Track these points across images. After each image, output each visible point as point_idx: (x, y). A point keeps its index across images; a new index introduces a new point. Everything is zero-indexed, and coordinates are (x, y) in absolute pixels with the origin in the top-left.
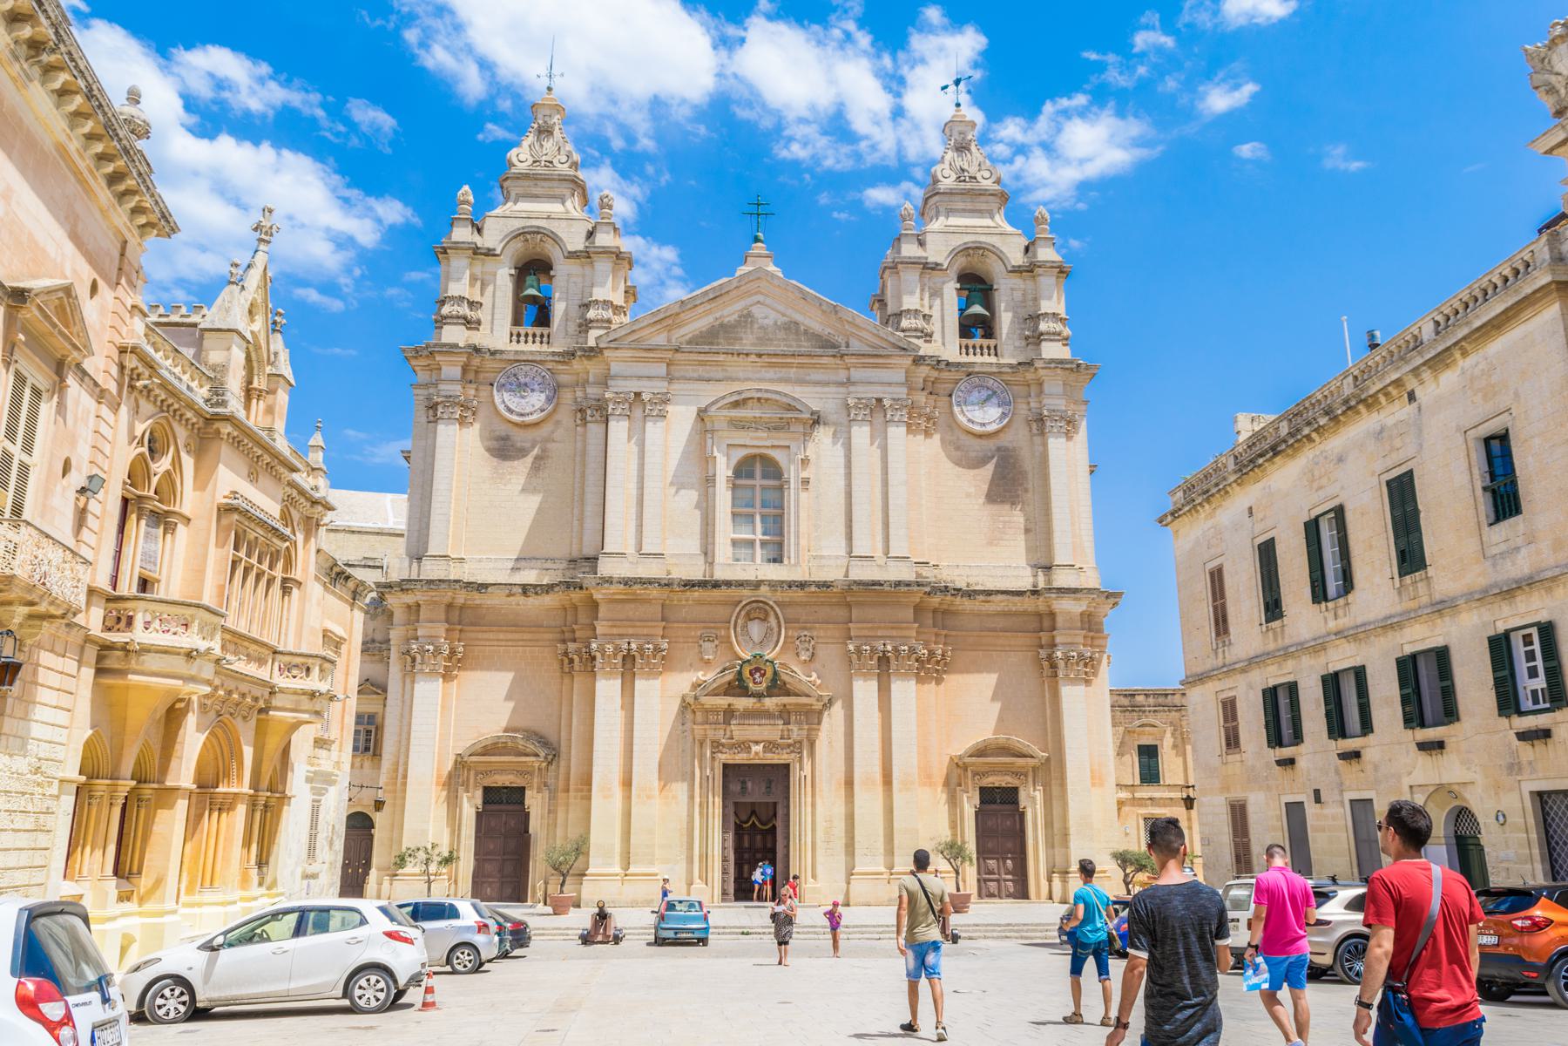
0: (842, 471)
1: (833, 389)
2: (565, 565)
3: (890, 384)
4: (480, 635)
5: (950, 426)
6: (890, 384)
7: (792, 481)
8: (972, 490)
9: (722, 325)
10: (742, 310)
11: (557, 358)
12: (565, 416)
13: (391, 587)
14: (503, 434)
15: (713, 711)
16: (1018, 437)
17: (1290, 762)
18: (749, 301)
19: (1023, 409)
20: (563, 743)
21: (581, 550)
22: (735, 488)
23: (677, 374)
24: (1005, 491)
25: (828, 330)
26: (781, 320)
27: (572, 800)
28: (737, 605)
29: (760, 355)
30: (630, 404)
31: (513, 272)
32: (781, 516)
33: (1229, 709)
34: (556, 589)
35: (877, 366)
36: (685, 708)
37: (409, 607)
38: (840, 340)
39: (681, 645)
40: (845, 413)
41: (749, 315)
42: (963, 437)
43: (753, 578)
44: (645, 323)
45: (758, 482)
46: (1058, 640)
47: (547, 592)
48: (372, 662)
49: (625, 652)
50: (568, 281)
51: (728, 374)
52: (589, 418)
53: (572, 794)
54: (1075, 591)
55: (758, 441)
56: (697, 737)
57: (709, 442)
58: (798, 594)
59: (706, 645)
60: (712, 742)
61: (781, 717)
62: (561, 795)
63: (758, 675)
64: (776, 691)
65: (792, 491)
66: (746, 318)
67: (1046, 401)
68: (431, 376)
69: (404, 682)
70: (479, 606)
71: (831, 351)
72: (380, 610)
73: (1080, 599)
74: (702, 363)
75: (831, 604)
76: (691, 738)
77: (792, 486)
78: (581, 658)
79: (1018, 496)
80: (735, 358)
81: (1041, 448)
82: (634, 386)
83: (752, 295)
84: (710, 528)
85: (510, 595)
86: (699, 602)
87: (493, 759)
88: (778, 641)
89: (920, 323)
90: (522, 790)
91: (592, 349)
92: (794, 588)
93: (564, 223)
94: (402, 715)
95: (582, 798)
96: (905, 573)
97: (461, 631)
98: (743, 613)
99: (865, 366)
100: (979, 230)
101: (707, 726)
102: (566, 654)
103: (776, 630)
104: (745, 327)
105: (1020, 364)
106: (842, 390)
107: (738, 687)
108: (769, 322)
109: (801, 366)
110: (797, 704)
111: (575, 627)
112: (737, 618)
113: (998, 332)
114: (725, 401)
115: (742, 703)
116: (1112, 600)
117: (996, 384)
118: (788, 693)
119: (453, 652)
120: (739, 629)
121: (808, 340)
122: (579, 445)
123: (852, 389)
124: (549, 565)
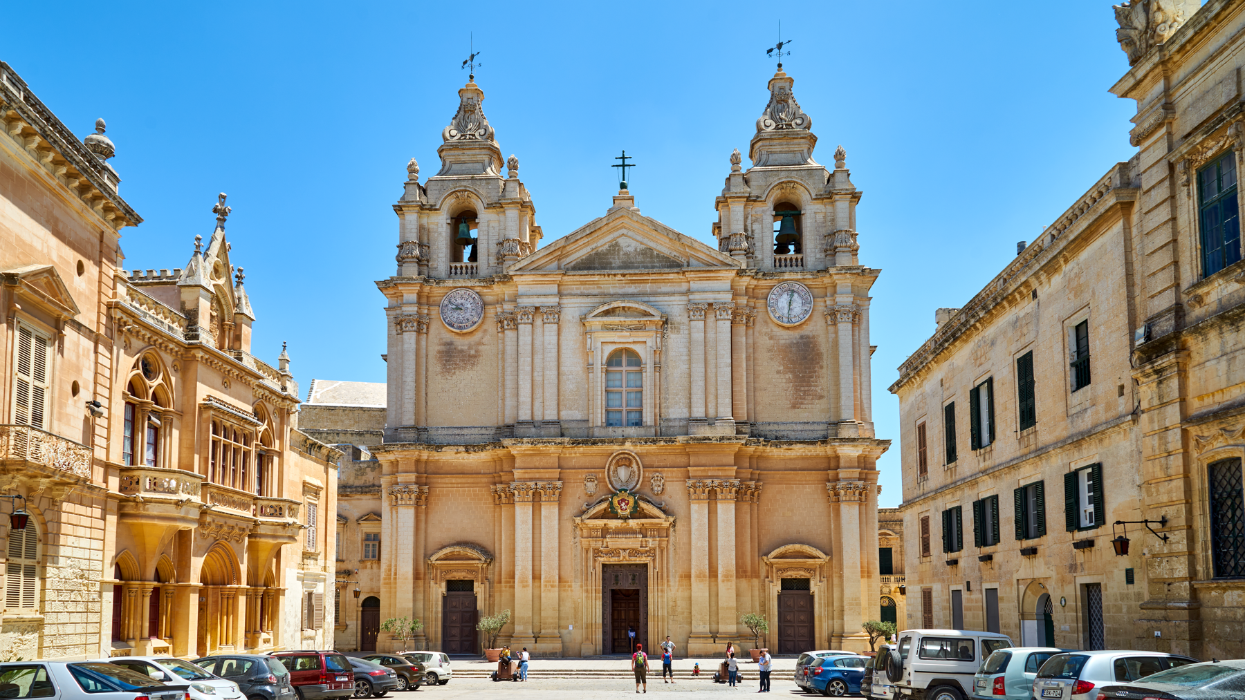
0: (686, 358)
1: (677, 298)
2: (493, 431)
3: (719, 292)
5: (766, 322)
6: (719, 292)
7: (648, 366)
8: (781, 368)
9: (597, 254)
10: (611, 241)
11: (482, 284)
12: (491, 326)
13: (379, 449)
14: (449, 341)
15: (595, 529)
16: (817, 328)
17: (988, 558)
18: (616, 234)
19: (820, 306)
20: (497, 551)
21: (504, 421)
22: (607, 372)
23: (565, 292)
24: (805, 368)
25: (675, 253)
26: (640, 247)
27: (503, 589)
28: (610, 456)
29: (624, 275)
30: (533, 316)
31: (449, 221)
32: (641, 392)
33: (925, 523)
34: (488, 448)
35: (709, 279)
36: (576, 527)
37: (392, 462)
38: (683, 260)
39: (573, 485)
40: (686, 315)
41: (617, 245)
42: (776, 329)
44: (541, 255)
45: (624, 368)
46: (841, 476)
47: (482, 450)
48: (374, 499)
51: (602, 290)
53: (503, 584)
54: (854, 440)
55: (623, 339)
56: (584, 546)
57: (589, 341)
58: (651, 448)
59: (589, 484)
60: (594, 550)
61: (640, 532)
62: (496, 585)
63: (624, 504)
64: (637, 515)
65: (648, 374)
66: (615, 247)
67: (837, 300)
68: (397, 301)
69: (392, 513)
70: (438, 461)
71: (676, 270)
72: (377, 465)
73: (857, 446)
74: (583, 283)
75: (675, 454)
76: (579, 547)
77: (648, 370)
78: (506, 495)
79: (815, 372)
80: (607, 278)
81: (833, 335)
82: (537, 301)
83: (618, 229)
84: (591, 403)
85: (457, 453)
86: (584, 455)
87: (451, 562)
88: (638, 481)
90: (472, 582)
91: (505, 276)
94: (392, 535)
95: (510, 587)
97: (426, 477)
98: (614, 461)
99: (701, 279)
101: (591, 539)
102: (496, 492)
103: (637, 473)
104: (614, 254)
105: (818, 272)
106: (684, 298)
108: (631, 249)
109: (654, 281)
110: (652, 524)
111: (501, 474)
112: (610, 465)
113: (804, 248)
114: (599, 311)
115: (614, 524)
116: (882, 447)
117: (801, 288)
118: (646, 516)
119: (421, 492)
120: (611, 473)
121: (660, 262)
122: (500, 346)
123: (691, 297)
124: (483, 431)
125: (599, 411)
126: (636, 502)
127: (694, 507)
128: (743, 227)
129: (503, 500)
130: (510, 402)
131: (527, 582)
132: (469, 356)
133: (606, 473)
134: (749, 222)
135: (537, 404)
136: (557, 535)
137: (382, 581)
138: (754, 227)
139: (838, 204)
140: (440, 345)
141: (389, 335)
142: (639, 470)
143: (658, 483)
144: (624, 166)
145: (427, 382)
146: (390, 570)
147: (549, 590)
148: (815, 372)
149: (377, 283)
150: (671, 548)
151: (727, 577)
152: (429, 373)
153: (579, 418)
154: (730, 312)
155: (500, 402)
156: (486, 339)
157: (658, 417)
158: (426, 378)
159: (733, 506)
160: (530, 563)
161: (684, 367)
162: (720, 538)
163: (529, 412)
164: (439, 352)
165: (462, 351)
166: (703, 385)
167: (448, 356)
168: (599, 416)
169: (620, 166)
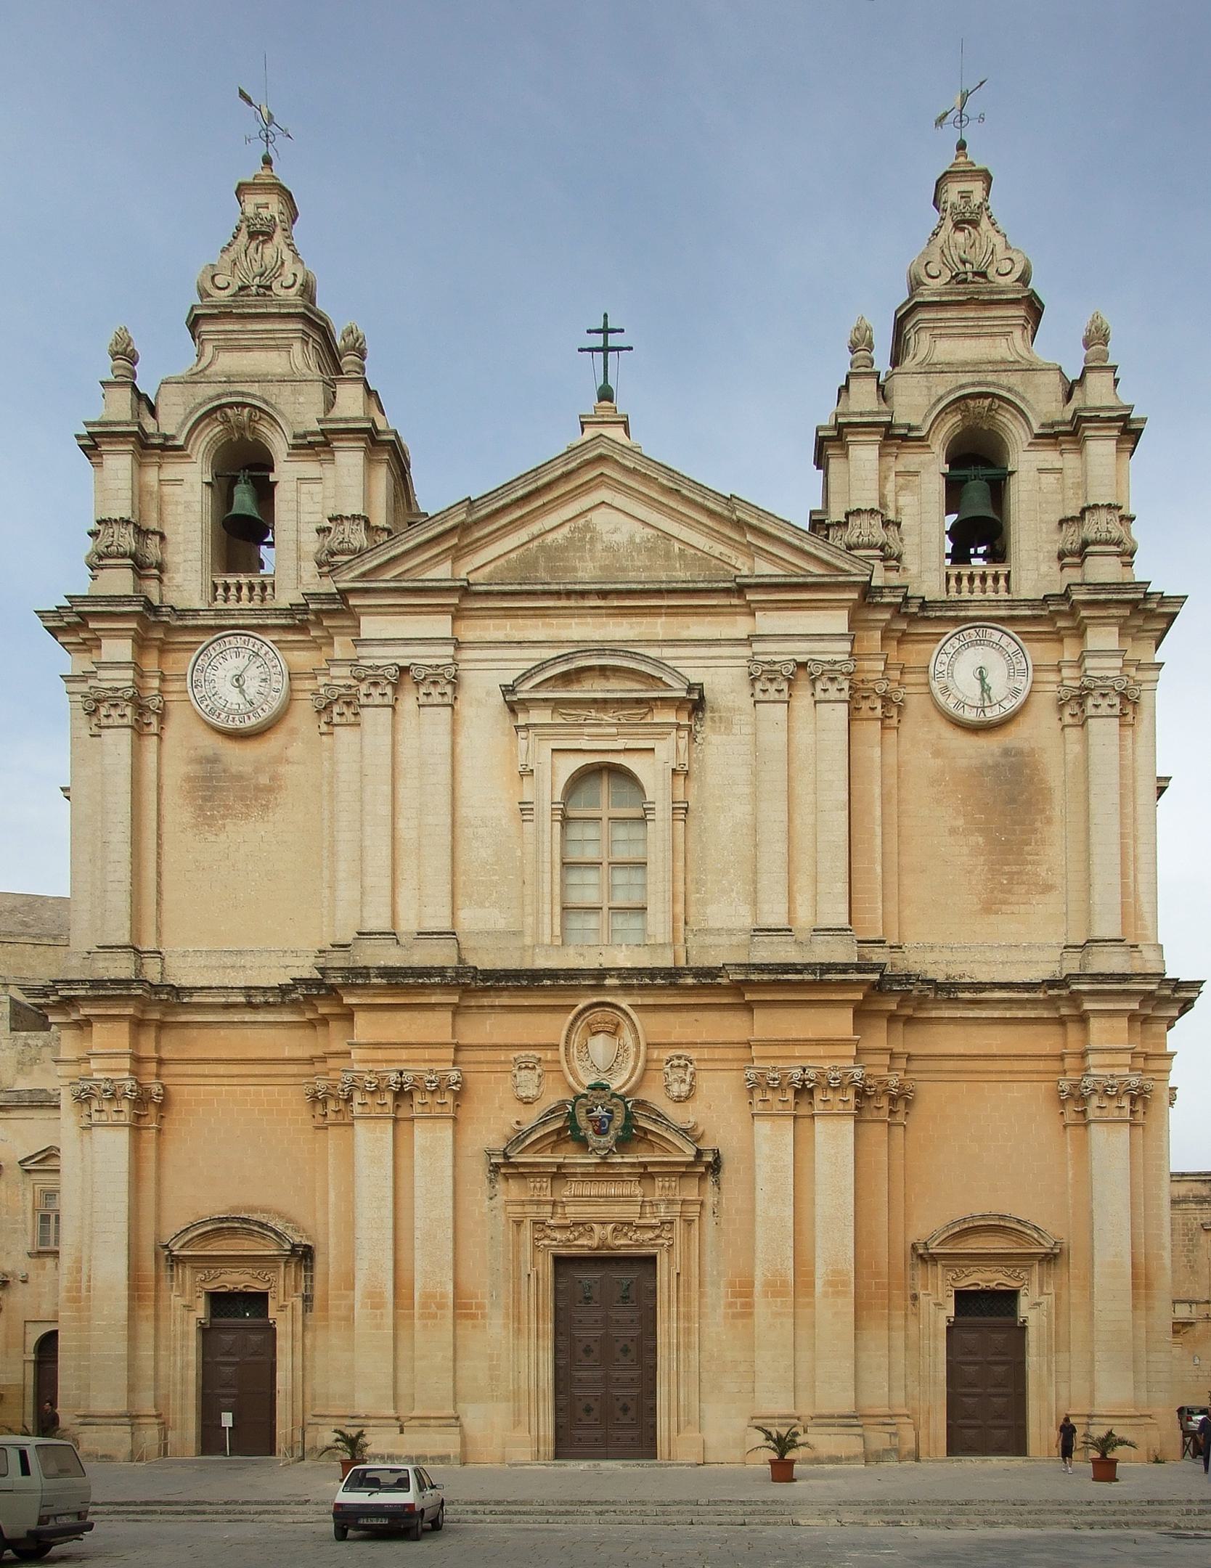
0: (747, 790)
4: (190, 1069)
7: (658, 807)
12: (303, 715)
14: (210, 753)
22: (566, 821)
40: (748, 691)
43: (597, 966)
45: (605, 811)
49: (395, 1088)
50: (298, 490)
52: (336, 719)
76: (502, 1218)
89: (879, 535)
92: (659, 981)
93: (287, 389)
96: (841, 952)
100: (984, 367)
103: (632, 1050)
105: (1046, 599)
107: (570, 1134)
112: (570, 1030)
120: (574, 1051)
125: (547, 908)
126: (629, 1116)
127: (763, 1128)
128: (876, 495)
129: (331, 1116)
130: (347, 892)
131: (381, 1294)
132: (258, 788)
133: (562, 1049)
134: (890, 487)
135: (405, 895)
136: (449, 1192)
137: (63, 1295)
138: (902, 501)
139: (1092, 446)
140: (191, 761)
141: (75, 739)
142: (638, 1045)
143: (681, 1072)
144: (606, 349)
145: (159, 846)
146: (79, 1270)
147: (434, 1316)
148: (1035, 831)
149: (42, 614)
150: (709, 1219)
151: (834, 1285)
152: (166, 828)
153: (501, 925)
154: (846, 685)
155: (327, 891)
156: (296, 750)
157: (681, 924)
158: (159, 837)
159: (849, 1124)
160: (390, 1253)
161: (741, 811)
162: (819, 1199)
163: (386, 912)
164: (188, 779)
165: (239, 777)
166: (785, 851)
167: (208, 788)
168: (547, 919)
169: (598, 350)
